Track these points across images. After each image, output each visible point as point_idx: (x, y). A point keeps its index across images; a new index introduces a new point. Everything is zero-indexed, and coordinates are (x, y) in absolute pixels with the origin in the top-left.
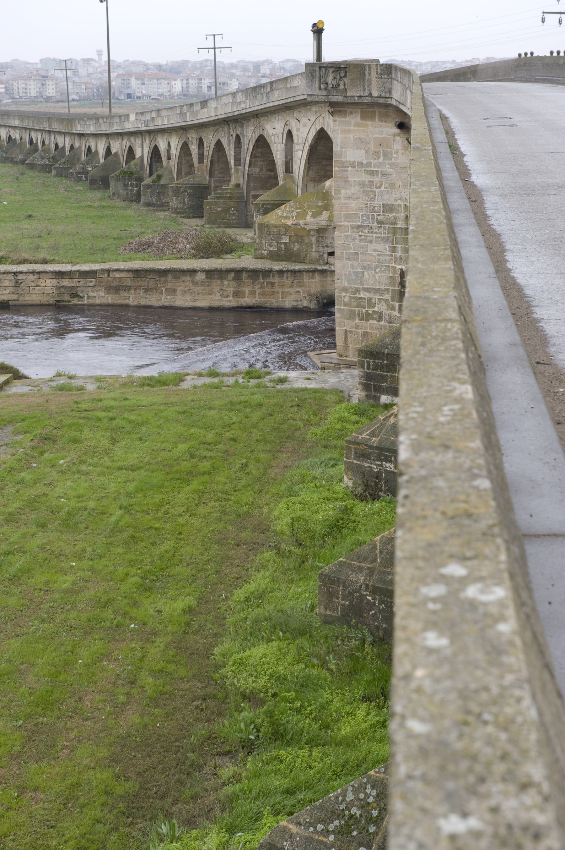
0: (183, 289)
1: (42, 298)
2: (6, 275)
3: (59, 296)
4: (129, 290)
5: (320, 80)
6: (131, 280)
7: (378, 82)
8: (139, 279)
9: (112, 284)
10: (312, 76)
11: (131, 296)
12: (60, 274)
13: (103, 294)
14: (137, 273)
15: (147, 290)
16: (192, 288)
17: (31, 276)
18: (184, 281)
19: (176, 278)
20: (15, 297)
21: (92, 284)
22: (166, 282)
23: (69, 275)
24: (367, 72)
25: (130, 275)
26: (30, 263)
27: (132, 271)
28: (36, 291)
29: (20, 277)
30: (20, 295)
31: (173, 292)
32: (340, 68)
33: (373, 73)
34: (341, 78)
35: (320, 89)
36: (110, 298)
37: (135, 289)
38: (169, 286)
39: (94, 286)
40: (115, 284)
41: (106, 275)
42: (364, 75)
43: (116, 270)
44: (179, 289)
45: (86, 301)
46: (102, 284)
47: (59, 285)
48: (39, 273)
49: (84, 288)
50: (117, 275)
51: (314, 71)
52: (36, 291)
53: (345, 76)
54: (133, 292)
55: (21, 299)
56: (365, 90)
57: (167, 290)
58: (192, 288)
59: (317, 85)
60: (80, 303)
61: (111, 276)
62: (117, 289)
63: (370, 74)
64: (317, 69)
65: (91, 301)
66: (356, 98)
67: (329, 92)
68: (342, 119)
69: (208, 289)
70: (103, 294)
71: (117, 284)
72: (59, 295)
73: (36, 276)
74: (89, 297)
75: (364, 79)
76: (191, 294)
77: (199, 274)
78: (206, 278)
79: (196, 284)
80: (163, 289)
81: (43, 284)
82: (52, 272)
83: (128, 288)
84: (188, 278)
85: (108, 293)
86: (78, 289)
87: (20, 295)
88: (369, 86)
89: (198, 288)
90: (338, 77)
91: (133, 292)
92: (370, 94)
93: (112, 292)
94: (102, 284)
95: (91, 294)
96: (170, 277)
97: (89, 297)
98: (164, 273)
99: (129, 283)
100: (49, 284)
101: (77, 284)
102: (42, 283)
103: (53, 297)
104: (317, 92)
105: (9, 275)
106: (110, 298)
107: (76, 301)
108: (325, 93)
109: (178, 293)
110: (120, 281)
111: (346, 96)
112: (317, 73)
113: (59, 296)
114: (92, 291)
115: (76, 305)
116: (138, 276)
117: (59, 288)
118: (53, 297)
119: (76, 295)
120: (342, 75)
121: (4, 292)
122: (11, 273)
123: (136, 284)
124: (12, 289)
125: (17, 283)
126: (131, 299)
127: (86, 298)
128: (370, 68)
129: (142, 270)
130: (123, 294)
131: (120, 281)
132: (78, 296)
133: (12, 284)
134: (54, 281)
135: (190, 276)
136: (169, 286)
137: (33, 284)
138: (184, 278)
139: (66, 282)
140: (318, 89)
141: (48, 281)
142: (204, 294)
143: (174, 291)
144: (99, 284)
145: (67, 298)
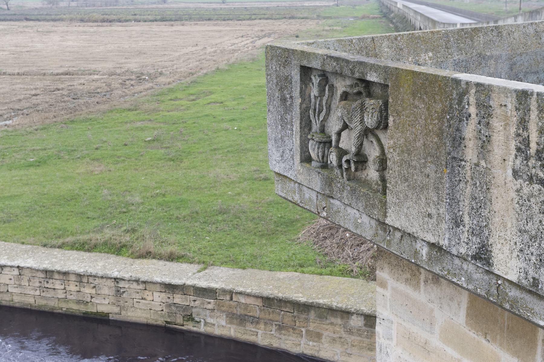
0: (332, 335)
1: (148, 316)
2: (105, 280)
3: (169, 316)
4: (258, 323)
5: (306, 125)
6: (261, 310)
7: (524, 202)
8: (271, 310)
9: (235, 312)
10: (283, 100)
11: (260, 332)
12: (170, 288)
13: (224, 323)
14: (269, 302)
15: (281, 328)
16: (344, 335)
17: (135, 285)
18: (332, 324)
19: (321, 317)
20: (116, 310)
21: (210, 306)
22: (307, 320)
23: (182, 290)
24: (469, 130)
25: (259, 302)
26: (154, 258)
27: (262, 298)
28: (141, 306)
29: (122, 284)
30: (122, 308)
31: (318, 336)
32: (368, 84)
33: (498, 138)
34: (366, 132)
35: (307, 159)
36: (232, 330)
37: (266, 324)
38: (312, 327)
39: (213, 310)
40: (239, 311)
41: (228, 297)
42: (458, 141)
43: (240, 293)
44: (325, 333)
45: (202, 329)
46: (223, 309)
47: (170, 301)
48: (144, 282)
49: (201, 310)
50: (243, 300)
51: (288, 79)
52: (141, 306)
53: (383, 124)
54: (262, 326)
55: (123, 313)
56: (457, 222)
57: (308, 331)
58: (344, 335)
59: (297, 141)
60: (195, 329)
61: (234, 299)
62: (242, 319)
63: (485, 145)
64: (296, 75)
65: (209, 330)
66: (425, 251)
67: (329, 182)
68: (402, 287)
69: (367, 341)
70: (224, 323)
71: (243, 312)
72: (170, 314)
73: (141, 286)
74: (206, 324)
75: (455, 161)
76: (343, 344)
77: (354, 317)
78: (365, 325)
79: (350, 332)
80: (303, 330)
81: (150, 298)
82: (161, 284)
83: (256, 321)
84: (339, 321)
85: (231, 323)
86: (194, 310)
87: (122, 308)
88: (480, 205)
89: (353, 338)
90: (356, 128)
91: (262, 326)
92: (483, 256)
93: (235, 321)
94: (223, 309)
95: (209, 320)
96: (312, 314)
97: (206, 324)
98: (306, 307)
99: (257, 314)
100: (158, 298)
101: (192, 304)
102: (148, 295)
103: (163, 316)
104: (296, 170)
105: (109, 280)
106: (232, 330)
107: (189, 326)
108: (317, 182)
109: (323, 340)
110: (246, 309)
111: (382, 224)
112: (296, 93)
113: (169, 316)
114: (211, 317)
115: (190, 332)
116: (270, 306)
117: (169, 306)
118: (163, 316)
119: (190, 318)
120: (370, 121)
121: (104, 302)
122: (112, 278)
123: (267, 316)
124: (112, 299)
125: (119, 292)
126: (259, 336)
127: (202, 324)
128: (486, 111)
129: (273, 299)
130: (250, 327)
131: (246, 309)
132: (193, 320)
133: (112, 292)
134: (163, 295)
135: (342, 318)
136: (312, 327)
137: (138, 296)
138: (333, 320)
139: (178, 299)
140: (297, 158)
141: (156, 295)
142: (361, 348)
143: (318, 336)
144: (219, 307)
145: (179, 320)
